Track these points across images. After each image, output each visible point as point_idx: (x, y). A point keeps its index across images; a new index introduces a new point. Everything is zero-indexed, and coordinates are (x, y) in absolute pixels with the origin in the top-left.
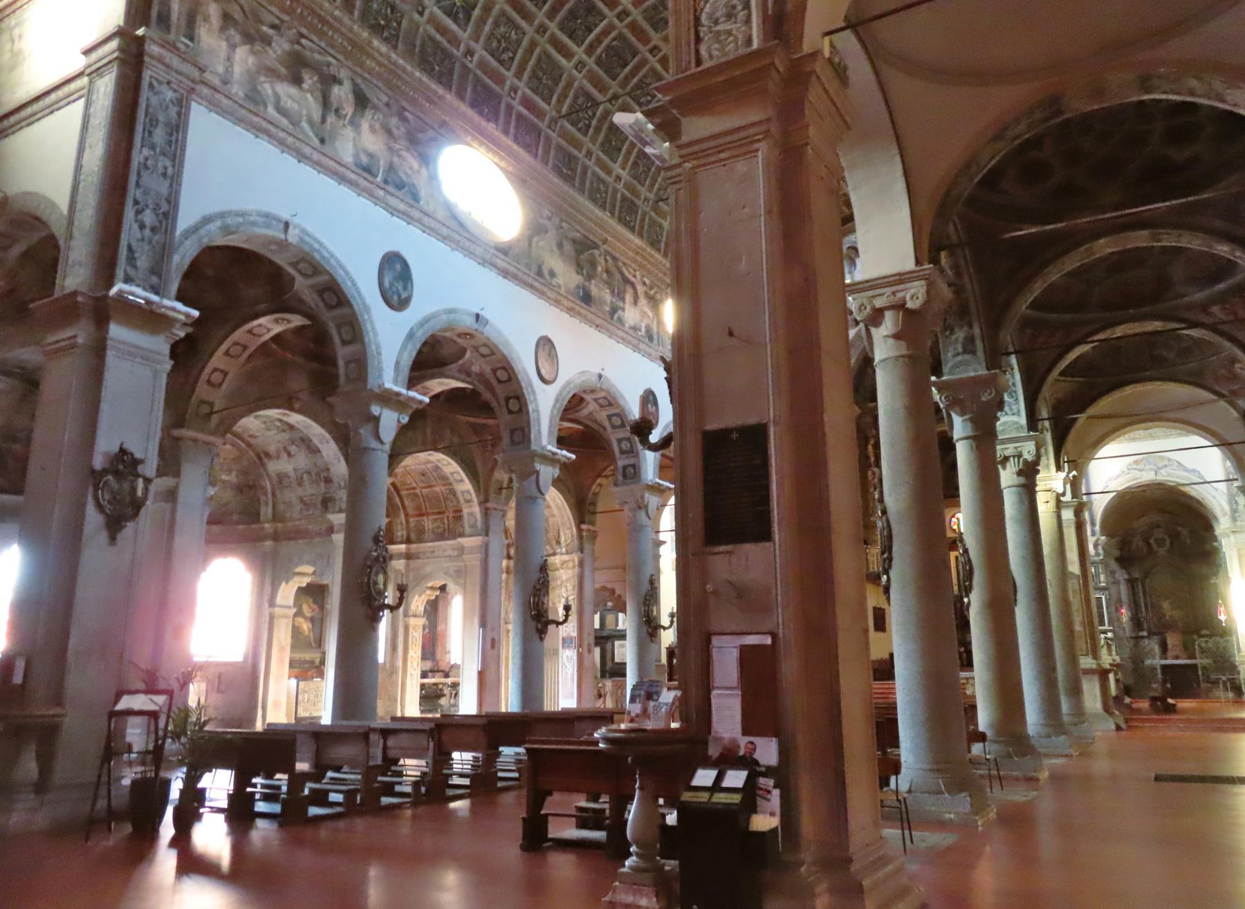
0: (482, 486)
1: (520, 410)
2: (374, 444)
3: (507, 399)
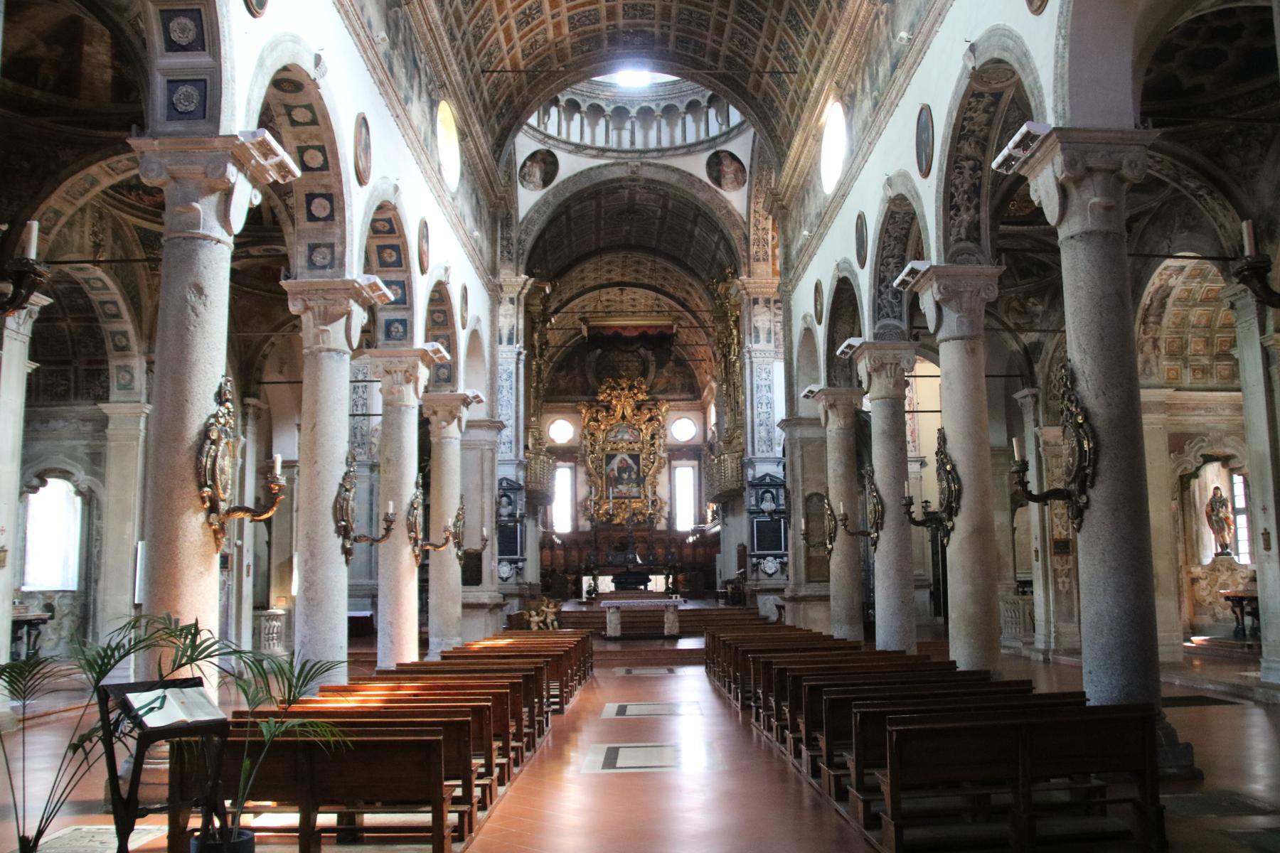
0: (145, 326)
1: (330, 217)
2: (218, 231)
3: (310, 197)
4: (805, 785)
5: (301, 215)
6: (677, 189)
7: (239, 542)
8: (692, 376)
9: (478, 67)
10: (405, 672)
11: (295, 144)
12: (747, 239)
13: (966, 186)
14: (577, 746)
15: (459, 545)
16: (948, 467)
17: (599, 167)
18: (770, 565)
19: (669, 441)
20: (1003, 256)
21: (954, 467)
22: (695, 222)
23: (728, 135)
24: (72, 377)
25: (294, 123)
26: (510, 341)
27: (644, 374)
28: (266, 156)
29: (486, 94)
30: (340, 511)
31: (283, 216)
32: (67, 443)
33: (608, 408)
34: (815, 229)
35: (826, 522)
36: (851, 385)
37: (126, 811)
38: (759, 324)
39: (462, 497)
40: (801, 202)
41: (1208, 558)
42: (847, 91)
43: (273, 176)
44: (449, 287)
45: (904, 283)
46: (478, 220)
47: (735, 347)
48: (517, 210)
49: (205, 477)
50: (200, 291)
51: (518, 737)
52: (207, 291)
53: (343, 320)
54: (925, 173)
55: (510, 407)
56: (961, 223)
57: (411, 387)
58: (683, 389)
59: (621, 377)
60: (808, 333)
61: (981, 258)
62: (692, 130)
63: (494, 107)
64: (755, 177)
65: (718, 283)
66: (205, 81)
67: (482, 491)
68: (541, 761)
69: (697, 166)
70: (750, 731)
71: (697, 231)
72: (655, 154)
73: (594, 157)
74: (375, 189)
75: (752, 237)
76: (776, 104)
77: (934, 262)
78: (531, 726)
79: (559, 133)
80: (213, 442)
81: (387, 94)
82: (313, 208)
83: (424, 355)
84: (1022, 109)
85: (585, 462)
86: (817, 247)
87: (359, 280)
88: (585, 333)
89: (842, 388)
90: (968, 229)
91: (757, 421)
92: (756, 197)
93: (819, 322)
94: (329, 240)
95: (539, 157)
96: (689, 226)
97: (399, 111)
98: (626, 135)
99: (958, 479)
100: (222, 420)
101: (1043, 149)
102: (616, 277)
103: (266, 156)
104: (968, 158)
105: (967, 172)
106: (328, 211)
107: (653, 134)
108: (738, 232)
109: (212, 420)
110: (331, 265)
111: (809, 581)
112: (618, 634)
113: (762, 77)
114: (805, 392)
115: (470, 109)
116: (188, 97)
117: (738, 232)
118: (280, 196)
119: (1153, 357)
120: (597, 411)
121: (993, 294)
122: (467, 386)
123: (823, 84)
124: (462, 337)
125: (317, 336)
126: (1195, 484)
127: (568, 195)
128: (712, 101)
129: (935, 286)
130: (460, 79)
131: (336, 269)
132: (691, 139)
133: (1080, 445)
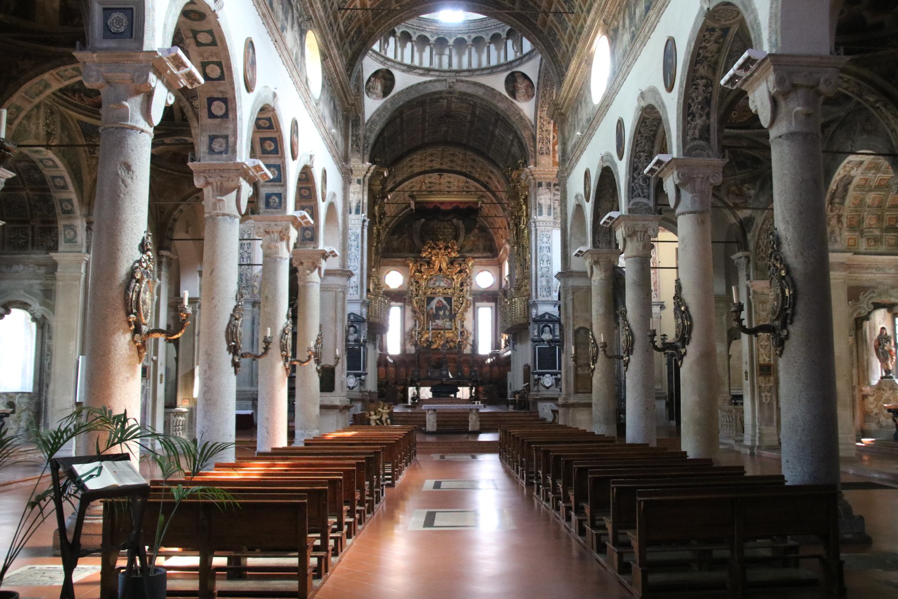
0: (86, 195)
1: (226, 115)
2: (142, 124)
3: (211, 100)
4: (573, 541)
5: (203, 113)
6: (482, 99)
7: (155, 358)
8: (491, 240)
9: (336, 5)
10: (277, 454)
11: (200, 60)
12: (534, 138)
13: (700, 98)
14: (404, 511)
15: (318, 362)
16: (683, 308)
17: (425, 82)
18: (548, 380)
19: (474, 287)
20: (727, 151)
21: (687, 308)
22: (495, 125)
23: (521, 60)
24: (30, 233)
25: (199, 44)
26: (357, 212)
27: (456, 238)
28: (178, 68)
29: (341, 26)
30: (231, 334)
31: (190, 114)
32: (26, 282)
33: (429, 263)
34: (585, 131)
35: (590, 349)
36: (610, 247)
37: (70, 552)
38: (542, 202)
39: (321, 326)
40: (576, 111)
41: (875, 380)
42: (612, 27)
43: (183, 82)
44: (313, 170)
45: (652, 171)
46: (335, 120)
47: (524, 218)
48: (363, 114)
49: (131, 306)
50: (128, 168)
51: (361, 503)
52: (133, 168)
53: (234, 193)
54: (670, 89)
55: (357, 261)
56: (695, 128)
57: (284, 244)
58: (485, 249)
59: (439, 240)
60: (579, 208)
61: (710, 153)
62: (495, 56)
63: (347, 37)
64: (541, 91)
65: (512, 170)
66: (132, 9)
67: (336, 322)
68: (378, 520)
69: (498, 83)
70: (533, 502)
71: (497, 132)
72: (467, 74)
73: (422, 75)
74: (259, 95)
75: (538, 137)
76: (558, 37)
77: (675, 155)
78: (371, 495)
79: (396, 56)
80: (138, 281)
81: (268, 24)
82: (213, 108)
83: (294, 220)
84: (745, 40)
85: (411, 302)
86: (587, 144)
87: (247, 163)
88: (413, 206)
89: (604, 250)
90: (700, 131)
91: (539, 273)
92: (542, 107)
93: (588, 200)
94: (225, 132)
95: (380, 74)
96: (491, 128)
97: (277, 37)
98: (445, 59)
99: (690, 317)
100: (144, 265)
101: (760, 70)
102: (437, 166)
103: (178, 68)
104: (702, 78)
105: (701, 88)
106: (224, 111)
107: (465, 59)
108: (528, 133)
109: (137, 265)
110: (226, 152)
111: (576, 392)
112: (434, 429)
113: (548, 16)
114: (576, 252)
115: (330, 37)
116: (119, 21)
117: (528, 133)
118: (188, 99)
119: (837, 229)
120: (421, 265)
121: (718, 180)
122: (326, 244)
123: (594, 21)
124: (322, 207)
125: (215, 204)
126: (867, 325)
127: (401, 103)
128: (510, 34)
129: (675, 173)
130: (322, 14)
131: (230, 153)
132: (494, 63)
133: (783, 292)
